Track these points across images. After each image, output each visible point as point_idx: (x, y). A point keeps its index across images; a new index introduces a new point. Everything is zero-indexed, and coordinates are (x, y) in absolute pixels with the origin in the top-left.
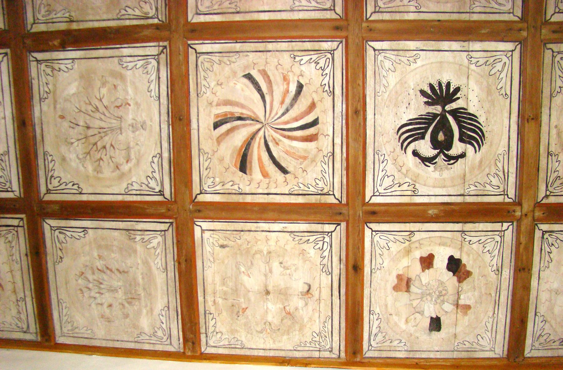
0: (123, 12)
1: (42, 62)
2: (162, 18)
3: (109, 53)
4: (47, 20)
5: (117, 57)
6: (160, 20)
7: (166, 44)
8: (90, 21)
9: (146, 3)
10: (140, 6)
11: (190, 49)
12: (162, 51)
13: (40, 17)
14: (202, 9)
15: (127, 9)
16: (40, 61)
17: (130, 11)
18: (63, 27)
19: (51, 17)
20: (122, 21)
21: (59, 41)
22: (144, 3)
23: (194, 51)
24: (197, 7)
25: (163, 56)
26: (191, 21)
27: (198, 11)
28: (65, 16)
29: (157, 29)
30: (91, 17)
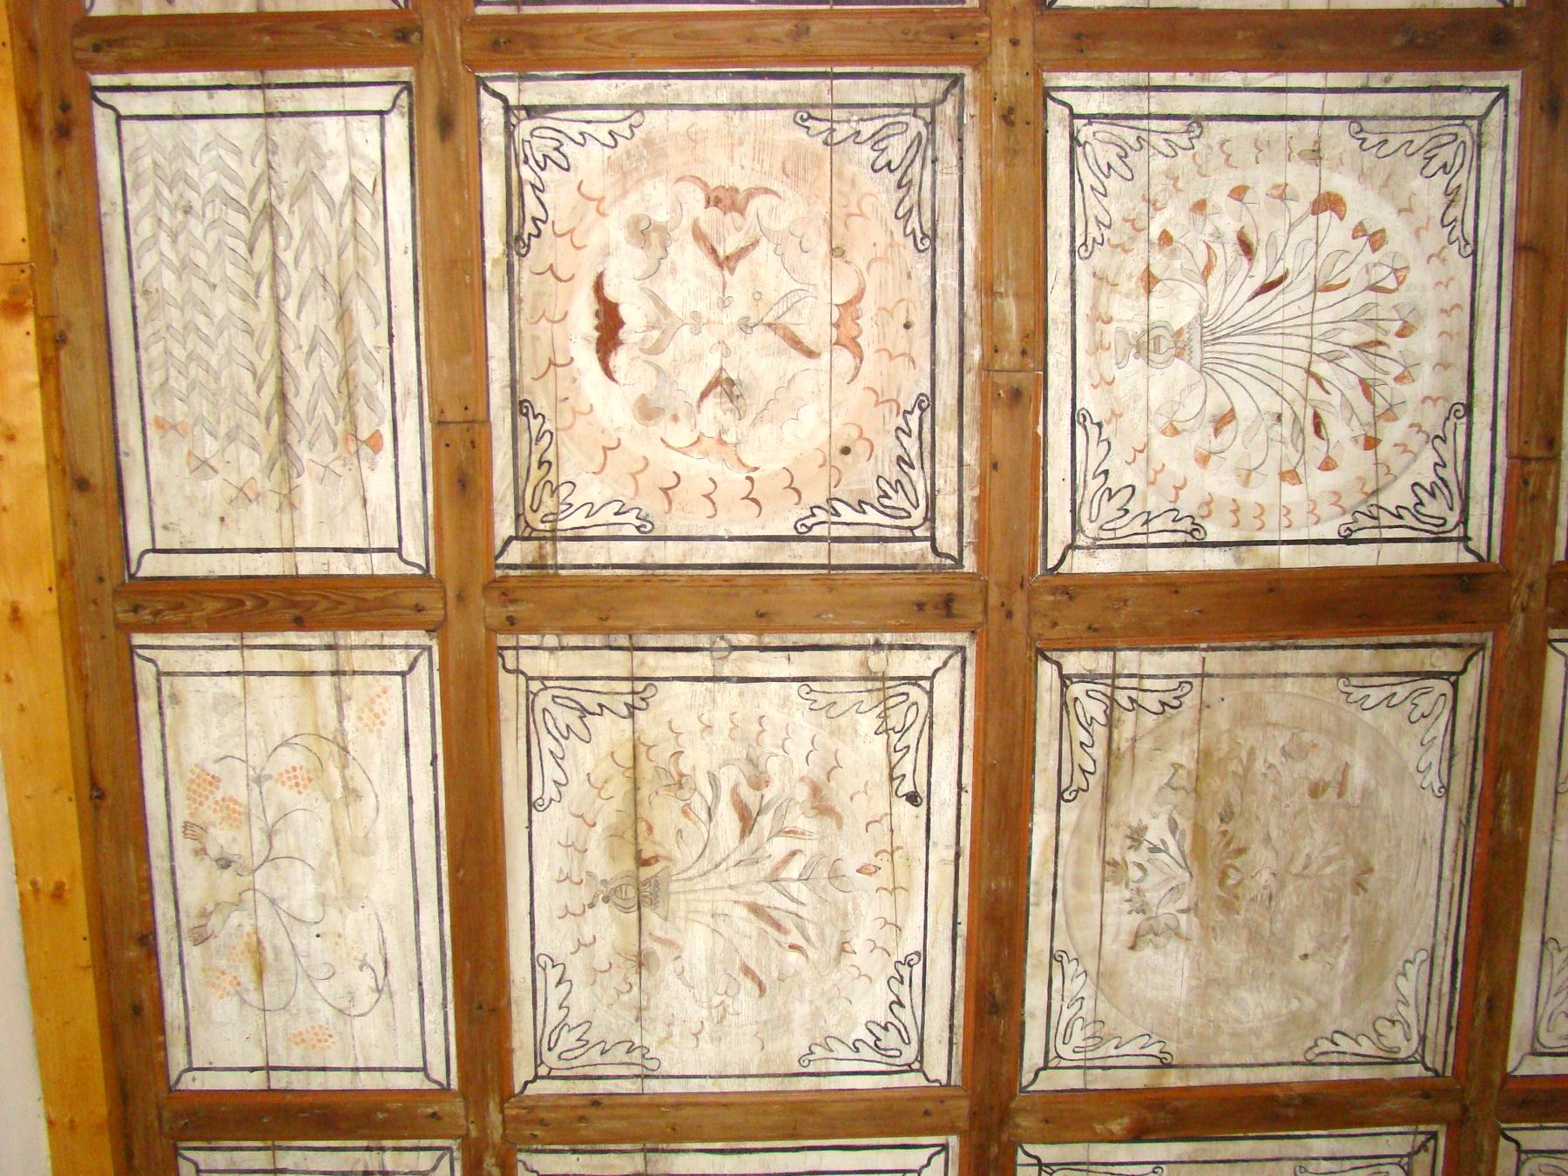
0: (1325, 1045)
1: (1054, 1168)
2: (1433, 1062)
3: (1269, 1148)
4: (1086, 1059)
5: (1290, 1159)
6: (1427, 1069)
7: (1434, 1127)
8: (1222, 1066)
9: (1393, 1022)
10: (1376, 1031)
11: (1503, 1142)
12: (1423, 1146)
13: (1065, 1051)
14: (1549, 1040)
15: (1337, 1037)
16: (1047, 1165)
17: (1345, 1044)
18: (1137, 1080)
19: (1101, 1052)
20: (1318, 1069)
21: (1126, 1121)
22: (1389, 1024)
23: (1513, 1145)
24: (1535, 1036)
25: (1424, 1158)
26: (1515, 1070)
27: (1537, 1045)
28: (1145, 1051)
29: (1426, 1095)
30: (1227, 1057)
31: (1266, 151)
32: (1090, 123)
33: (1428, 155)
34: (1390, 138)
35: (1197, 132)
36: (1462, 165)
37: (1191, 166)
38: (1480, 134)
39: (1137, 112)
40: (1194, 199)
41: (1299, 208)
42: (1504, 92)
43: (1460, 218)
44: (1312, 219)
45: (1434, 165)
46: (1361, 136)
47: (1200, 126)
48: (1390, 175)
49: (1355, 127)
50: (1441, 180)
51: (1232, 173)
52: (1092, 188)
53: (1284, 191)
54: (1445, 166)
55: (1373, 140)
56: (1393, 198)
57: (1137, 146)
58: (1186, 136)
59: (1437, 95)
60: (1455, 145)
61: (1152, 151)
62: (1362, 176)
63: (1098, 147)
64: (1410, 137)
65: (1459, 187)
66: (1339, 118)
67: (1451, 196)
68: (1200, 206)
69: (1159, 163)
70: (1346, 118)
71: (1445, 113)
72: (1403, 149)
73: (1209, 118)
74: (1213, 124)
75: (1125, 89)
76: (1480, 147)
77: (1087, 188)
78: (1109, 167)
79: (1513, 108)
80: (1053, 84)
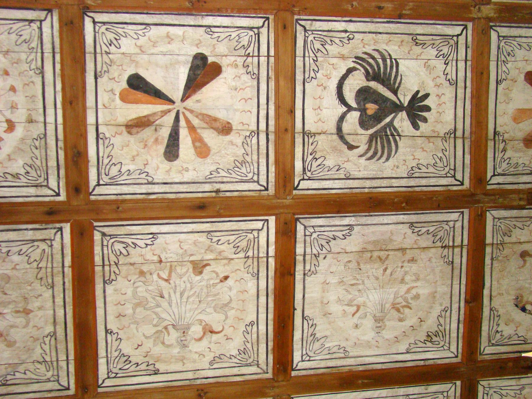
31: (31, 100)
32: (38, 28)
33: (32, 166)
34: (38, 150)
35: (37, 72)
36: (29, 180)
37: (23, 69)
38: (41, 186)
39: (44, 48)
40: (8, 70)
41: (8, 114)
42: (58, 195)
43: (7, 180)
44: (4, 120)
45: (29, 169)
46: (39, 139)
47: (40, 73)
48: (22, 150)
49: (42, 136)
50: (23, 172)
51: (21, 86)
52: (11, 28)
53: (15, 108)
54: (28, 173)
55: (37, 143)
56: (14, 152)
57: (30, 47)
58: (35, 67)
59: (56, 168)
60: (36, 176)
61: (28, 53)
62: (23, 140)
63: (29, 31)
64: (39, 158)
65: (20, 179)
66: (45, 130)
67: (16, 176)
68: (7, 73)
69: (23, 56)
70: (46, 133)
71: (49, 172)
72: (34, 155)
73: (43, 77)
74: (41, 79)
75: (53, 43)
76: (36, 186)
77: (11, 26)
78: (21, 35)
79: (52, 199)
80: (54, 14)
